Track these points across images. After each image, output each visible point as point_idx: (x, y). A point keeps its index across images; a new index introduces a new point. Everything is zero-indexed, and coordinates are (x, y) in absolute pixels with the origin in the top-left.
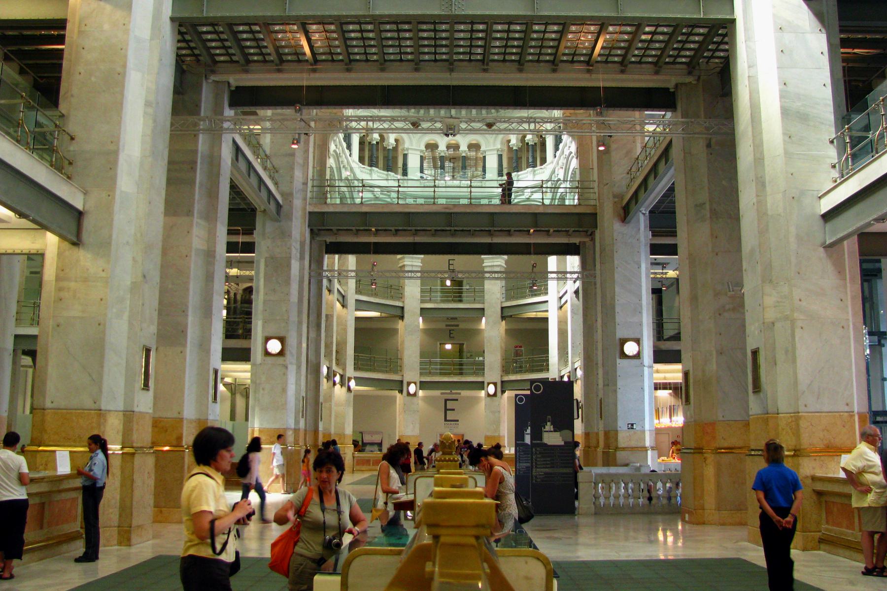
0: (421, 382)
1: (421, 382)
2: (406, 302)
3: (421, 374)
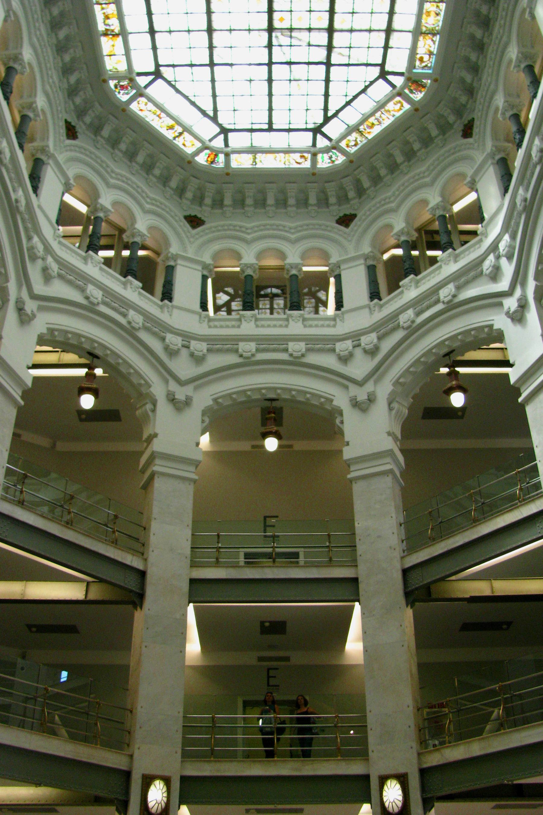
0: (184, 779)
2: (153, 556)
3: (186, 756)
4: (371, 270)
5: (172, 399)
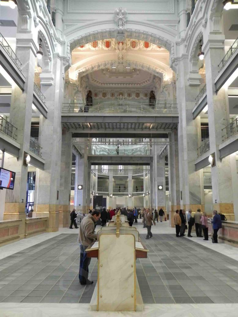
1: (113, 194)
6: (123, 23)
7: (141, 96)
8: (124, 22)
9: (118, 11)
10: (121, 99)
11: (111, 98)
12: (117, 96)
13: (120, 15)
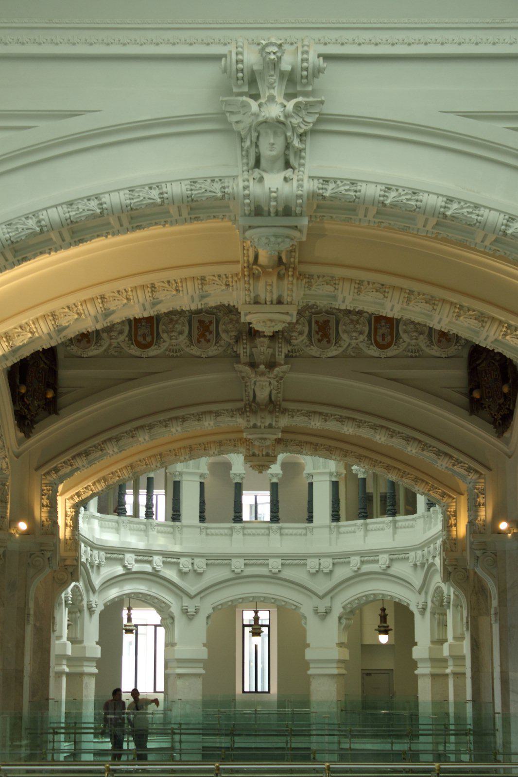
4: (335, 485)
5: (185, 612)
6: (288, 146)
7: (405, 337)
8: (296, 143)
9: (251, 58)
10: (262, 367)
11: (195, 351)
12: (237, 339)
13: (271, 86)
